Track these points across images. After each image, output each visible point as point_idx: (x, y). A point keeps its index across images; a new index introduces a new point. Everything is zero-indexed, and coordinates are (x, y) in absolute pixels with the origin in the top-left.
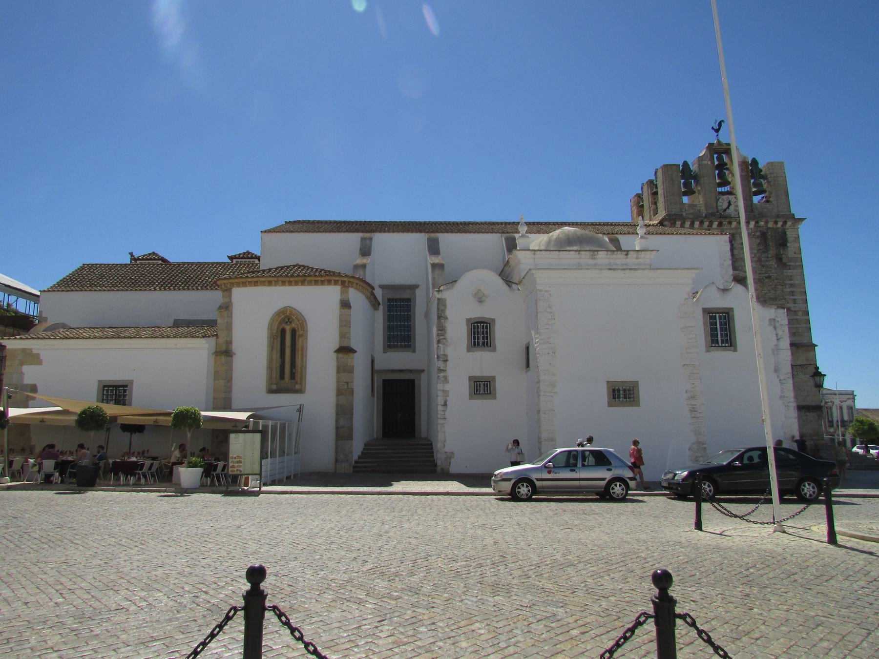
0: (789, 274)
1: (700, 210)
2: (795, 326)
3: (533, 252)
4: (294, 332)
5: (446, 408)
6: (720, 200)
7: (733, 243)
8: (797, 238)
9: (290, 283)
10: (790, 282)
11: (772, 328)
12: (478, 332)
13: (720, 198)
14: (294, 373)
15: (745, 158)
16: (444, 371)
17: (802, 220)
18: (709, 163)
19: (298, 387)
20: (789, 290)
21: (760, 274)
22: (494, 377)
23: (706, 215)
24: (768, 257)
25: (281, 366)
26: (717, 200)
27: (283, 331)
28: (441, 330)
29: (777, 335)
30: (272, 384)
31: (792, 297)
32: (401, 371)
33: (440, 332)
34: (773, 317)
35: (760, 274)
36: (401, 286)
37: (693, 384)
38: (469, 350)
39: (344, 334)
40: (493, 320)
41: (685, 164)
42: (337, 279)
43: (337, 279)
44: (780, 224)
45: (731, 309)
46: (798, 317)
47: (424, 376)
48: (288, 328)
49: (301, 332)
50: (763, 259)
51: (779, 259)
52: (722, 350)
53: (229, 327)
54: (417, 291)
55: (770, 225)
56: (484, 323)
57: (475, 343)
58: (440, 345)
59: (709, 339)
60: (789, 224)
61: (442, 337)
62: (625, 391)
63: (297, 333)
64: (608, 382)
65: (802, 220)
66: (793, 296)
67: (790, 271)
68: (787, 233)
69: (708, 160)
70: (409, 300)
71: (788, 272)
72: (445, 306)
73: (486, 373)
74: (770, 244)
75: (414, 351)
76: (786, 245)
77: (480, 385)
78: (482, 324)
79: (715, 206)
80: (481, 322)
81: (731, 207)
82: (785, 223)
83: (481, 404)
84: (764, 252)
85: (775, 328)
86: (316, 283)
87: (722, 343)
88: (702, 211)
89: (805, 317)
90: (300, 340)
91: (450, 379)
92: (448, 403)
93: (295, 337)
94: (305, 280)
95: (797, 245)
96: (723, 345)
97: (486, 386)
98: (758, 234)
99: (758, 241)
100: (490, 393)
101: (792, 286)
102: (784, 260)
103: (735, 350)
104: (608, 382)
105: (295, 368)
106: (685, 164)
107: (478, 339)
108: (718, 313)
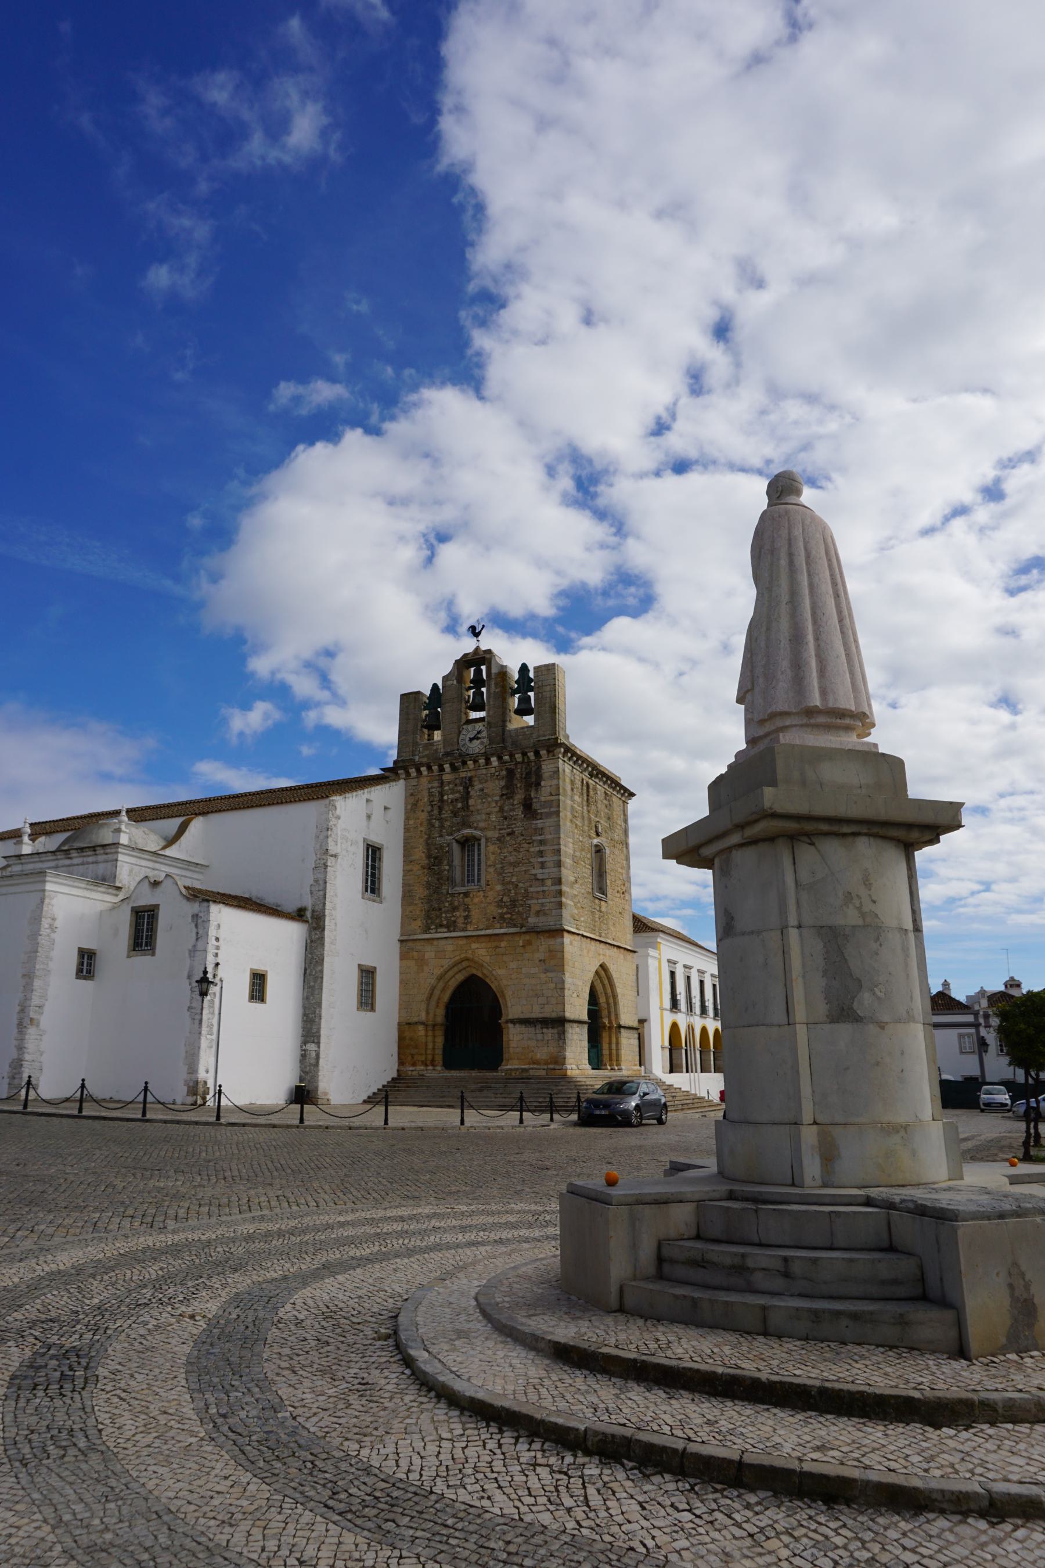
0: (540, 826)
2: (540, 901)
6: (464, 732)
10: (539, 838)
11: (193, 925)
18: (455, 682)
20: (537, 849)
24: (513, 805)
26: (460, 732)
31: (540, 860)
34: (196, 912)
44: (531, 755)
46: (545, 888)
50: (506, 808)
51: (528, 806)
59: (132, 942)
60: (543, 752)
68: (543, 767)
71: (539, 823)
82: (537, 754)
84: (508, 798)
85: (196, 926)
87: (146, 945)
89: (557, 887)
95: (554, 782)
98: (504, 773)
99: (503, 783)
101: (542, 842)
102: (535, 806)
103: (153, 954)
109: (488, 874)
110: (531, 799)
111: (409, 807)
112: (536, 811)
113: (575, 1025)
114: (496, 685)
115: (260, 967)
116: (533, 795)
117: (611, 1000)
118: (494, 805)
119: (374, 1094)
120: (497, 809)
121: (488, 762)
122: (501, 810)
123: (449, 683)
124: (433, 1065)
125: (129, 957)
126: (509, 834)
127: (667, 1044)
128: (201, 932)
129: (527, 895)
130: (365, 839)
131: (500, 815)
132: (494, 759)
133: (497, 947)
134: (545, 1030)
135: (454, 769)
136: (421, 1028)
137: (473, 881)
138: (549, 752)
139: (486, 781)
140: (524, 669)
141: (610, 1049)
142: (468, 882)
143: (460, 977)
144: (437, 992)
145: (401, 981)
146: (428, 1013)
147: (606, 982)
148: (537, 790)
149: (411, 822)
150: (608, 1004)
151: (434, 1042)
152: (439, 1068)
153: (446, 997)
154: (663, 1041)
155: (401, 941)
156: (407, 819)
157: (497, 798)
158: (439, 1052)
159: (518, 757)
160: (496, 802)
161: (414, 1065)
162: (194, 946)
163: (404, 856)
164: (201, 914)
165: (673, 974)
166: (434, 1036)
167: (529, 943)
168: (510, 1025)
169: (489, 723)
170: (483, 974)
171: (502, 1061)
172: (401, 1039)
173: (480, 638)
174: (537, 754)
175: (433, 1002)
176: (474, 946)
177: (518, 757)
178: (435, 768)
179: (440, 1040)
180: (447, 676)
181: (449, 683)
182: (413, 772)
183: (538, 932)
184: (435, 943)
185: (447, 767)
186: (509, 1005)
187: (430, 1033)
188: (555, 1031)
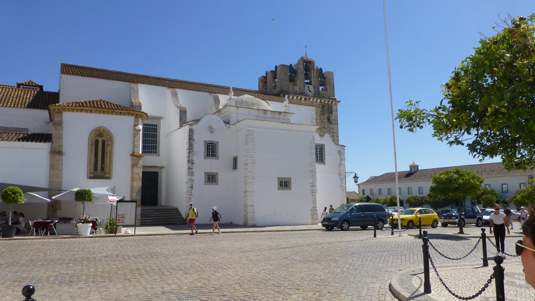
0: (332, 127)
3: (237, 108)
4: (103, 142)
5: (193, 189)
8: (337, 110)
9: (104, 113)
11: (339, 155)
12: (210, 148)
13: (306, 86)
14: (104, 167)
16: (192, 169)
17: (339, 102)
18: (302, 67)
19: (107, 175)
21: (320, 126)
22: (217, 173)
23: (299, 93)
25: (95, 162)
26: (304, 87)
27: (97, 142)
28: (191, 146)
29: (341, 158)
30: (91, 173)
32: (151, 167)
33: (190, 147)
34: (339, 150)
35: (320, 126)
36: (152, 117)
37: (313, 180)
38: (205, 158)
39: (135, 146)
40: (218, 142)
41: (291, 65)
42: (133, 112)
43: (133, 112)
44: (330, 103)
45: (324, 145)
47: (164, 170)
48: (100, 140)
49: (110, 143)
50: (322, 119)
51: (329, 119)
52: (320, 164)
53: (60, 137)
54: (162, 121)
55: (326, 102)
56: (213, 144)
57: (208, 154)
58: (190, 154)
60: (334, 103)
61: (191, 150)
62: (285, 182)
63: (106, 143)
64: (278, 178)
65: (339, 102)
66: (333, 137)
70: (156, 126)
72: (193, 133)
73: (213, 171)
74: (326, 112)
75: (159, 156)
77: (210, 177)
78: (212, 145)
79: (303, 89)
80: (211, 143)
81: (308, 91)
82: (332, 102)
83: (211, 187)
84: (323, 115)
86: (121, 114)
87: (319, 160)
90: (108, 147)
91: (195, 173)
92: (193, 187)
93: (104, 145)
94: (114, 111)
97: (213, 177)
98: (321, 106)
99: (321, 109)
100: (215, 182)
102: (331, 120)
103: (324, 164)
104: (278, 178)
105: (104, 164)
106: (291, 65)
107: (210, 152)
110: (329, 117)
112: (331, 122)
114: (316, 73)
120: (319, 118)
122: (321, 119)
126: (323, 128)
128: (342, 157)
131: (320, 120)
135: (305, 99)
148: (331, 115)
157: (319, 114)
160: (319, 116)
162: (340, 163)
164: (341, 151)
169: (314, 86)
174: (332, 102)
185: (303, 99)
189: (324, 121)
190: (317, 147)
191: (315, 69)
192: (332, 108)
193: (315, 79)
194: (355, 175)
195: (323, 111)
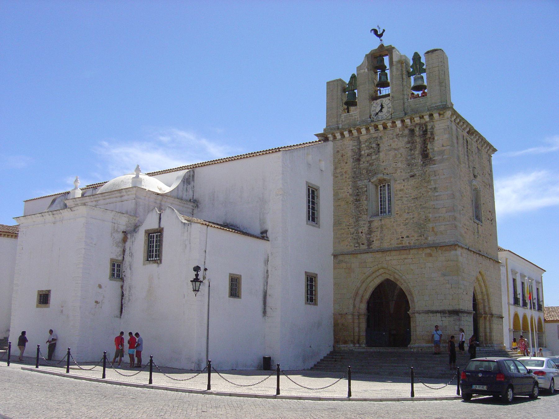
1: (355, 119)
6: (374, 105)
7: (380, 146)
15: (401, 56)
18: (366, 70)
31: (436, 194)
44: (427, 118)
51: (425, 155)
59: (146, 255)
60: (436, 116)
67: (436, 166)
68: (435, 125)
69: (366, 67)
71: (435, 167)
74: (418, 140)
76: (434, 139)
82: (431, 115)
87: (156, 257)
88: (356, 120)
96: (156, 259)
98: (406, 132)
99: (406, 139)
102: (431, 155)
108: (156, 233)
109: (397, 206)
111: (336, 160)
113: (465, 315)
114: (397, 69)
115: (236, 272)
116: (429, 147)
117: (486, 297)
118: (400, 156)
119: (318, 362)
121: (394, 122)
123: (362, 71)
124: (358, 343)
125: (144, 264)
127: (512, 327)
129: (427, 220)
130: (307, 182)
132: (399, 124)
133: (406, 259)
134: (444, 319)
136: (350, 317)
137: (385, 212)
138: (440, 114)
139: (393, 138)
140: (416, 57)
141: (485, 332)
142: (381, 213)
143: (378, 281)
144: (361, 292)
145: (335, 284)
146: (354, 306)
147: (483, 284)
149: (338, 171)
150: (483, 300)
151: (359, 327)
152: (364, 346)
153: (367, 296)
154: (510, 326)
155: (335, 256)
156: (336, 168)
157: (403, 151)
158: (363, 333)
159: (417, 120)
161: (345, 342)
163: (334, 195)
165: (514, 280)
166: (359, 323)
167: (430, 255)
168: (417, 315)
169: (393, 97)
170: (395, 278)
171: (410, 340)
172: (336, 325)
173: (382, 38)
174: (431, 115)
175: (358, 299)
176: (388, 258)
177: (417, 120)
178: (355, 132)
179: (364, 326)
180: (360, 66)
181: (362, 71)
182: (338, 136)
183: (437, 247)
184: (359, 256)
186: (416, 300)
187: (356, 321)
188: (451, 319)
189: (413, 161)
190: (153, 234)
191: (394, 63)
192: (433, 129)
193: (394, 83)
194: (195, 277)
195: (412, 142)
